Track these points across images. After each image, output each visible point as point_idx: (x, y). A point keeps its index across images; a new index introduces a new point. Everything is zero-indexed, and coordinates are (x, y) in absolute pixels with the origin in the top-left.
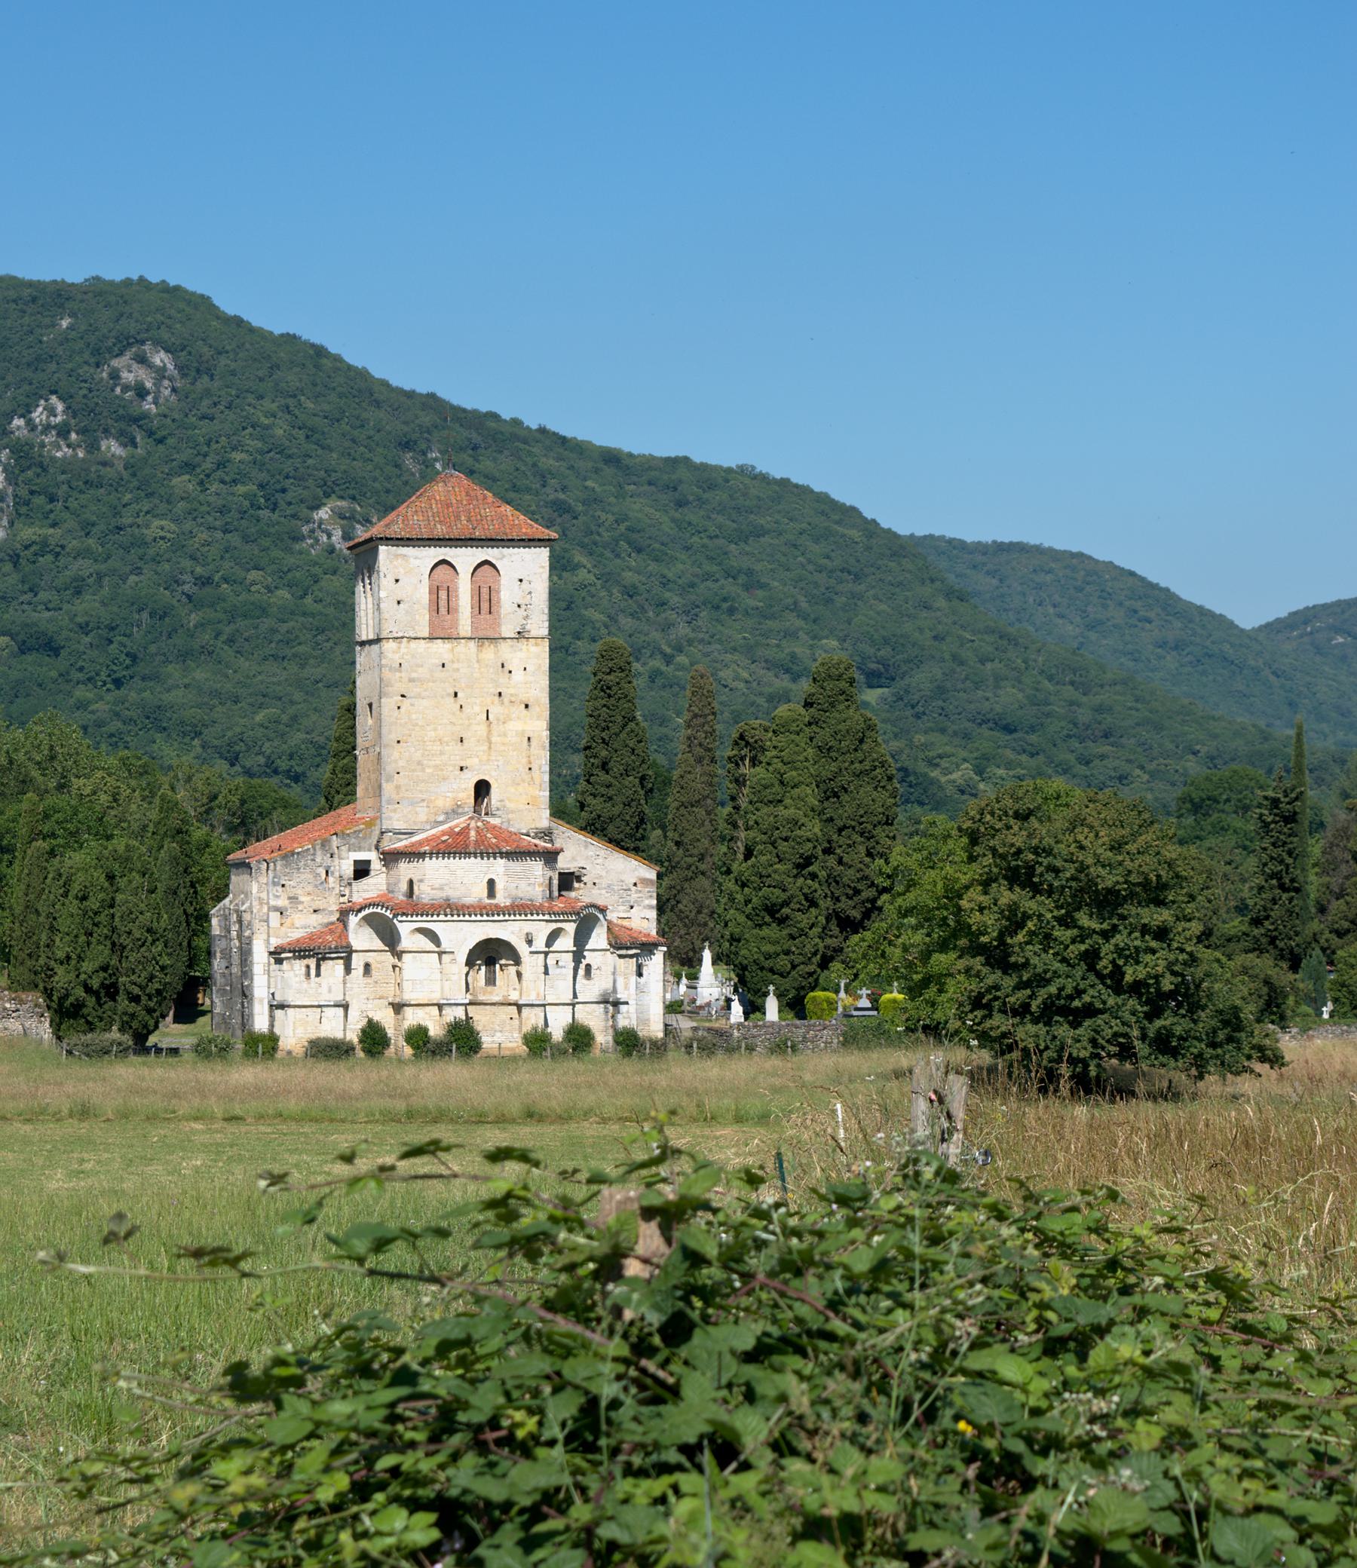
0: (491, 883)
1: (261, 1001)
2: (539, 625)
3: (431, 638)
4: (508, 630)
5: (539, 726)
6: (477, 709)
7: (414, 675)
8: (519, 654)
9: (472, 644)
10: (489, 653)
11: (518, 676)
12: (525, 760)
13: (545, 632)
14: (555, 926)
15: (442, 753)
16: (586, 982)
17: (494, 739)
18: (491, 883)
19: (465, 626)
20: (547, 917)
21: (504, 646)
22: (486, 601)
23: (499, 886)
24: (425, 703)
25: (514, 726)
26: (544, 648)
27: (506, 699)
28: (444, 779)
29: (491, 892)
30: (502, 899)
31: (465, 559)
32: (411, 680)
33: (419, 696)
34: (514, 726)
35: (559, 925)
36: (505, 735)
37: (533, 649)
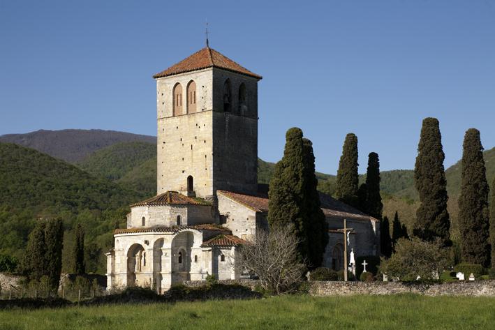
0: (144, 218)
1: (455, 227)
2: (210, 106)
3: (174, 116)
4: (199, 110)
5: (208, 149)
6: (188, 145)
7: (168, 133)
8: (203, 119)
9: (187, 117)
10: (193, 120)
11: (202, 129)
12: (204, 166)
13: (211, 108)
14: (159, 237)
15: (177, 165)
16: (195, 264)
17: (194, 157)
18: (144, 218)
19: (184, 111)
20: (153, 233)
21: (197, 116)
22: (191, 98)
23: (146, 220)
24: (171, 145)
25: (201, 151)
26: (212, 112)
27: (198, 139)
28: (178, 177)
29: (144, 224)
30: (147, 226)
31: (184, 80)
32: (167, 136)
33: (169, 142)
34: (201, 151)
35: (162, 236)
36: (198, 155)
37: (208, 116)
